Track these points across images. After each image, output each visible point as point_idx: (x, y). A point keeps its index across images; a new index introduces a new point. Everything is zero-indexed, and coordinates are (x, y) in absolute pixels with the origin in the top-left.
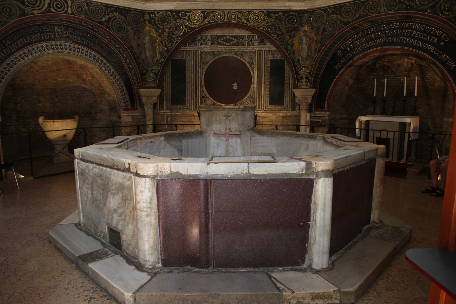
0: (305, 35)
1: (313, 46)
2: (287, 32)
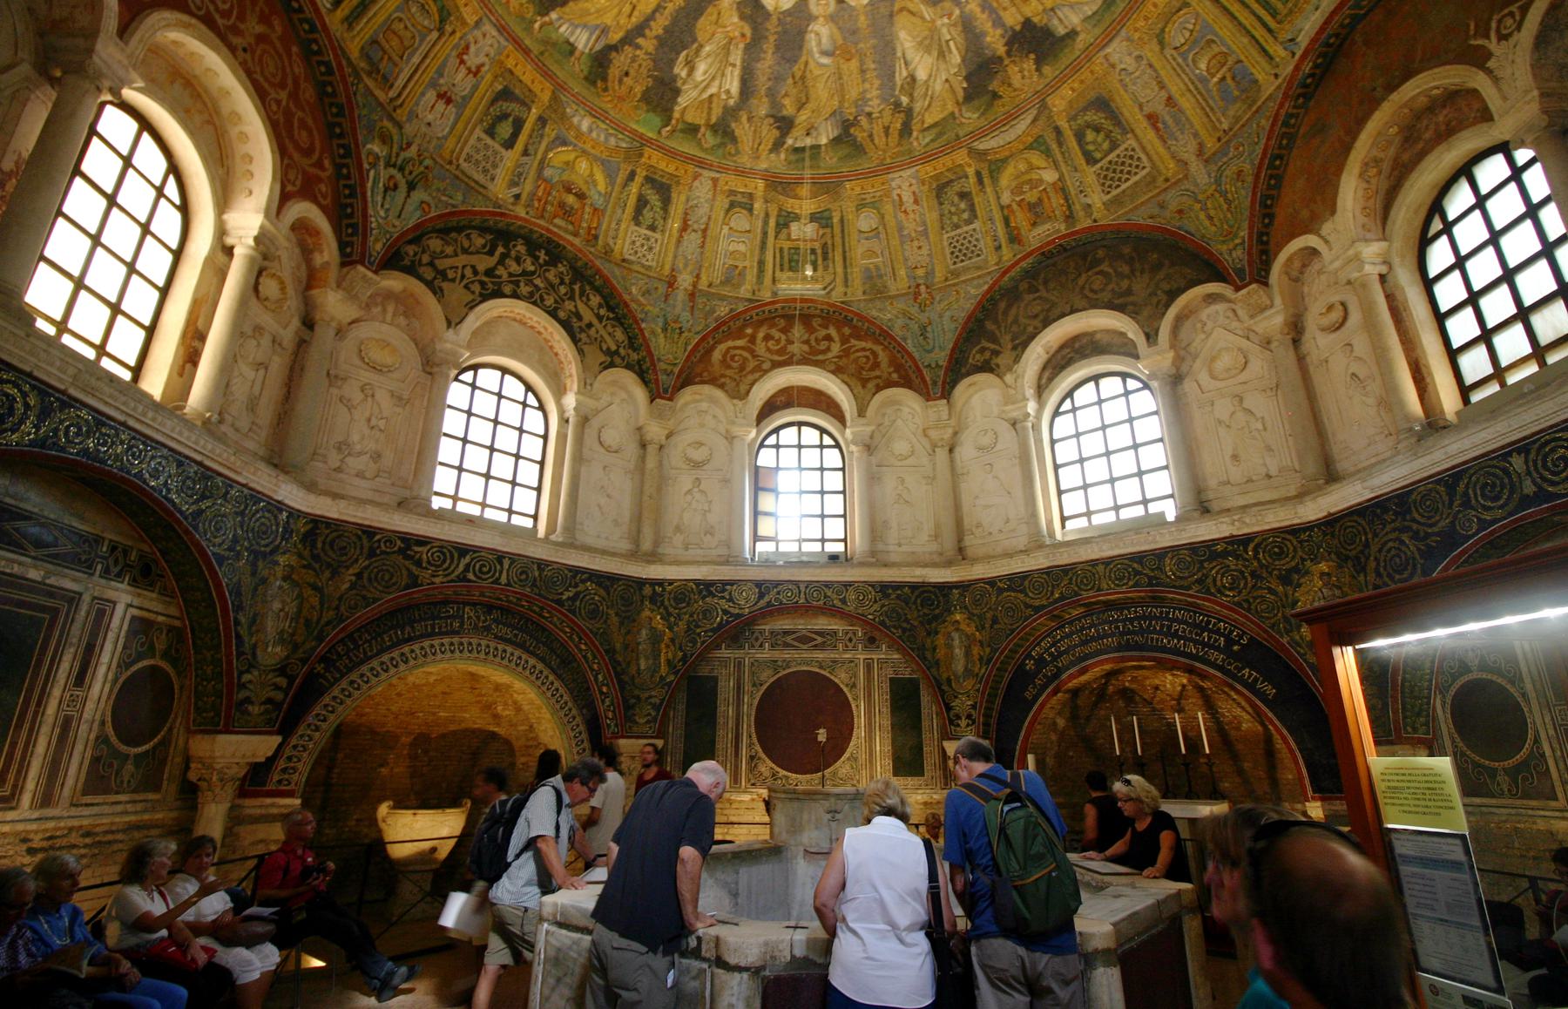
0: (957, 630)
1: (976, 650)
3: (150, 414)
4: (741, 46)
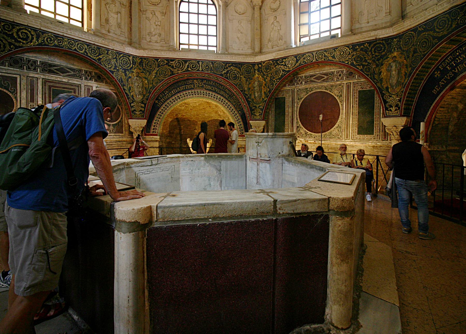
0: (394, 61)
2: (374, 61)
3: (69, 31)
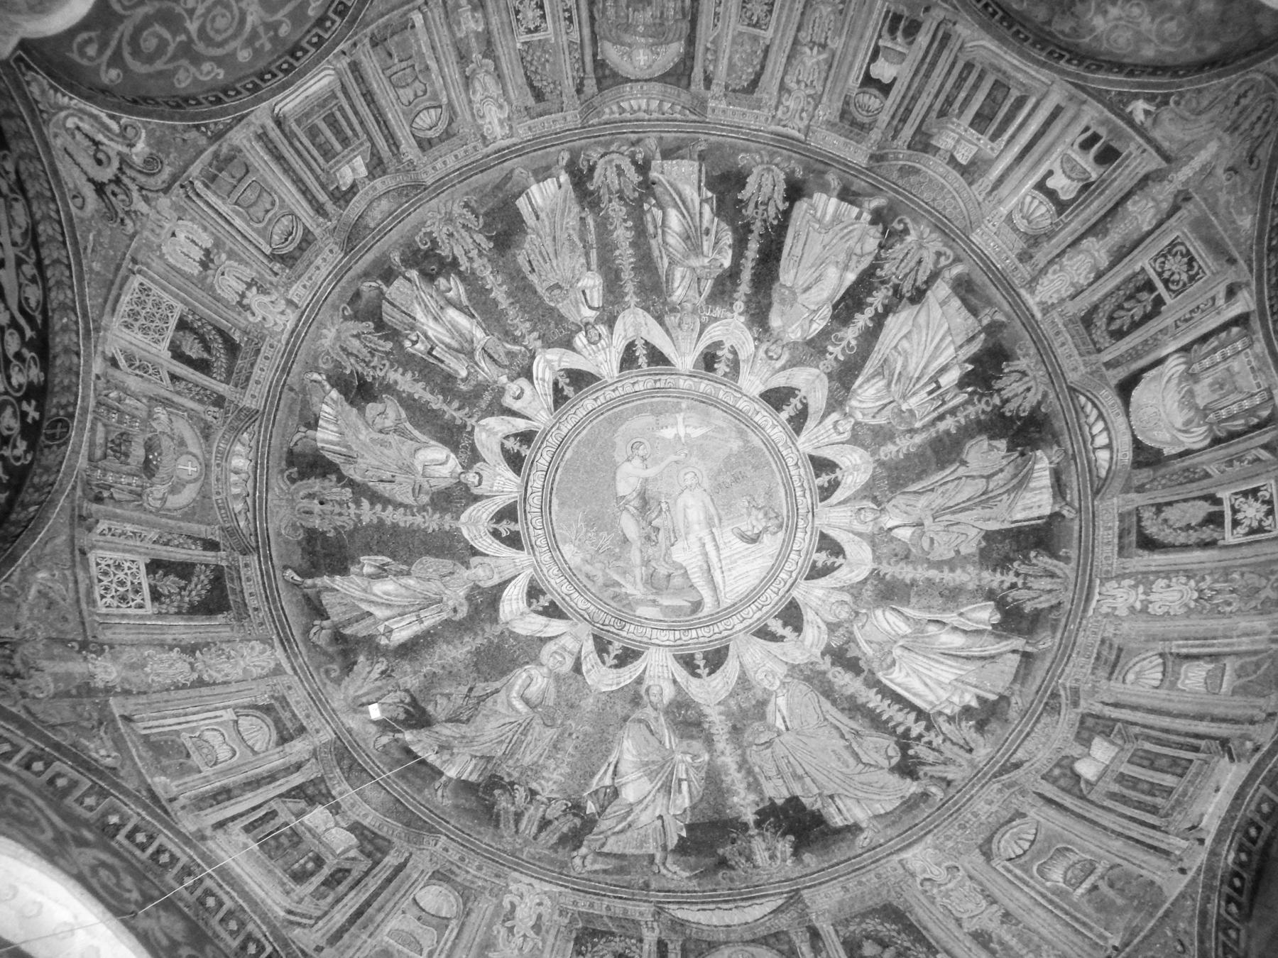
4: (444, 616)
